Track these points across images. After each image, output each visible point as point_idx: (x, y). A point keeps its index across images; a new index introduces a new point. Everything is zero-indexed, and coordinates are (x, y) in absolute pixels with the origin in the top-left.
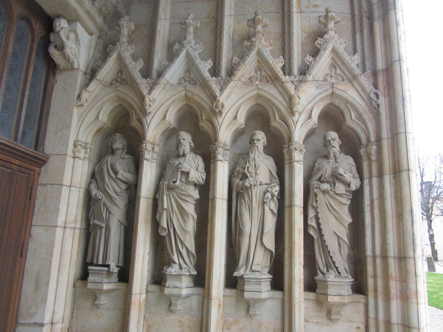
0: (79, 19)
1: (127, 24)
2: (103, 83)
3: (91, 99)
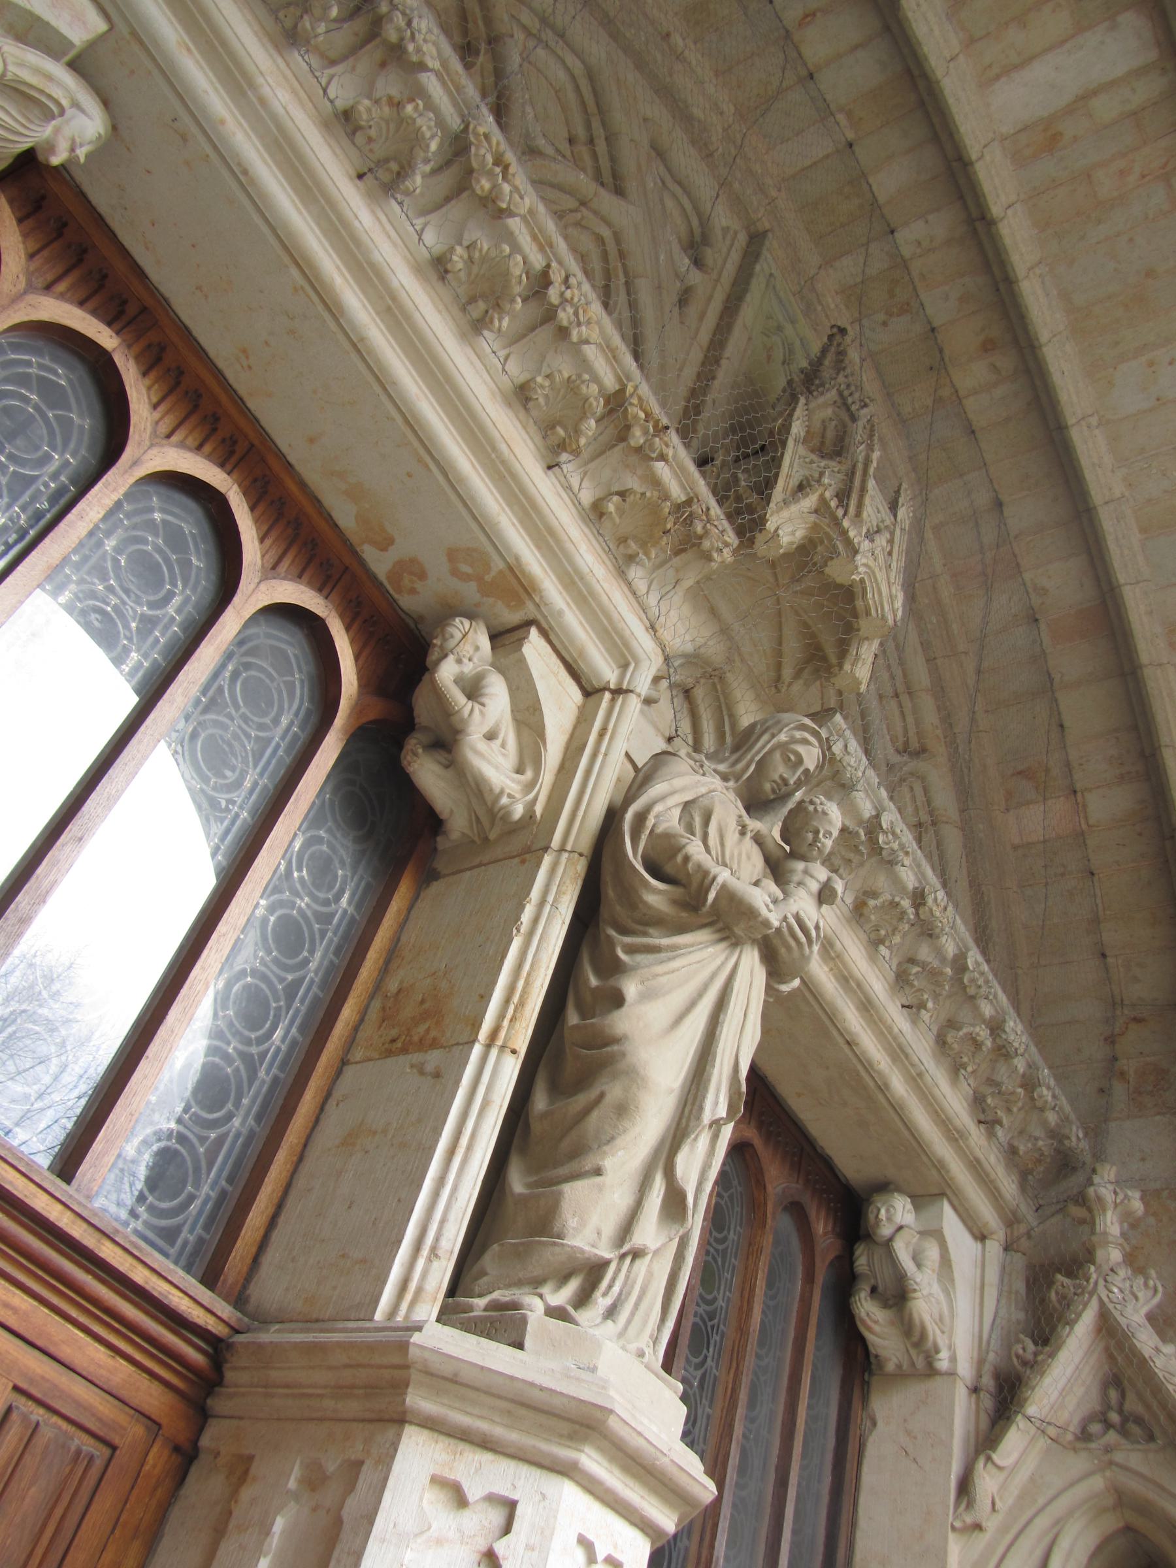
0: (949, 1192)
1: (1115, 1193)
2: (1052, 1431)
3: (1010, 1501)
